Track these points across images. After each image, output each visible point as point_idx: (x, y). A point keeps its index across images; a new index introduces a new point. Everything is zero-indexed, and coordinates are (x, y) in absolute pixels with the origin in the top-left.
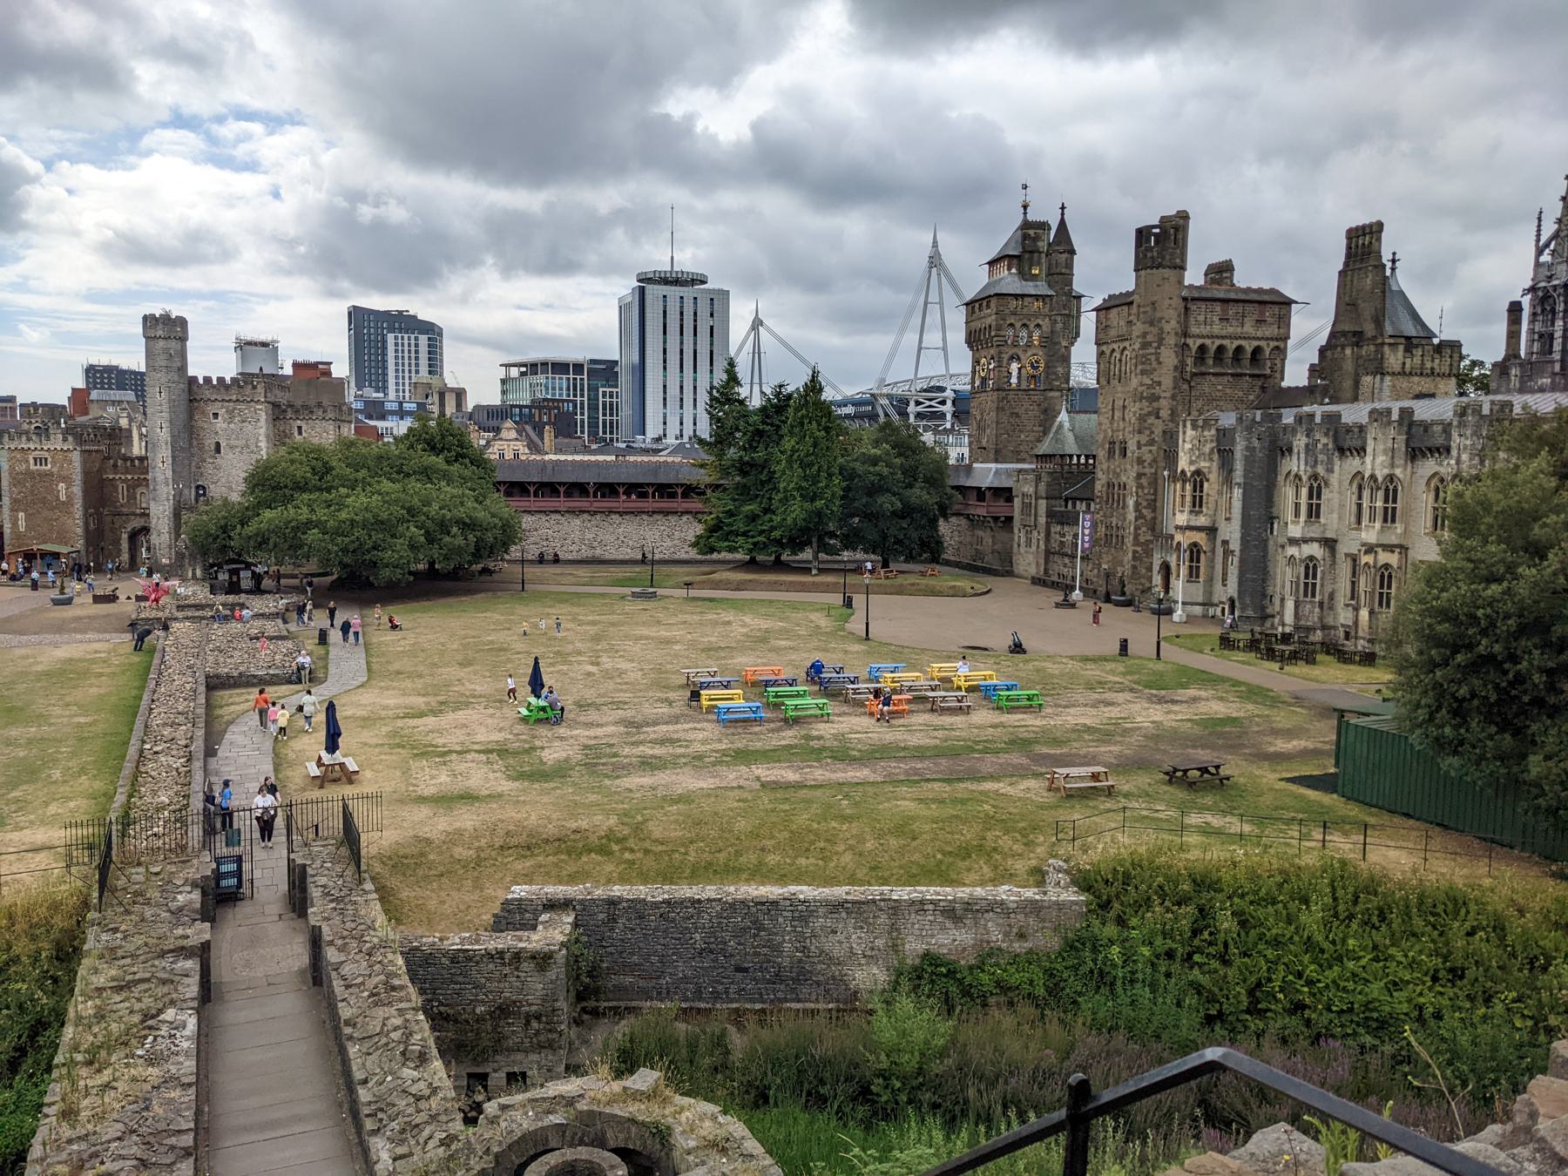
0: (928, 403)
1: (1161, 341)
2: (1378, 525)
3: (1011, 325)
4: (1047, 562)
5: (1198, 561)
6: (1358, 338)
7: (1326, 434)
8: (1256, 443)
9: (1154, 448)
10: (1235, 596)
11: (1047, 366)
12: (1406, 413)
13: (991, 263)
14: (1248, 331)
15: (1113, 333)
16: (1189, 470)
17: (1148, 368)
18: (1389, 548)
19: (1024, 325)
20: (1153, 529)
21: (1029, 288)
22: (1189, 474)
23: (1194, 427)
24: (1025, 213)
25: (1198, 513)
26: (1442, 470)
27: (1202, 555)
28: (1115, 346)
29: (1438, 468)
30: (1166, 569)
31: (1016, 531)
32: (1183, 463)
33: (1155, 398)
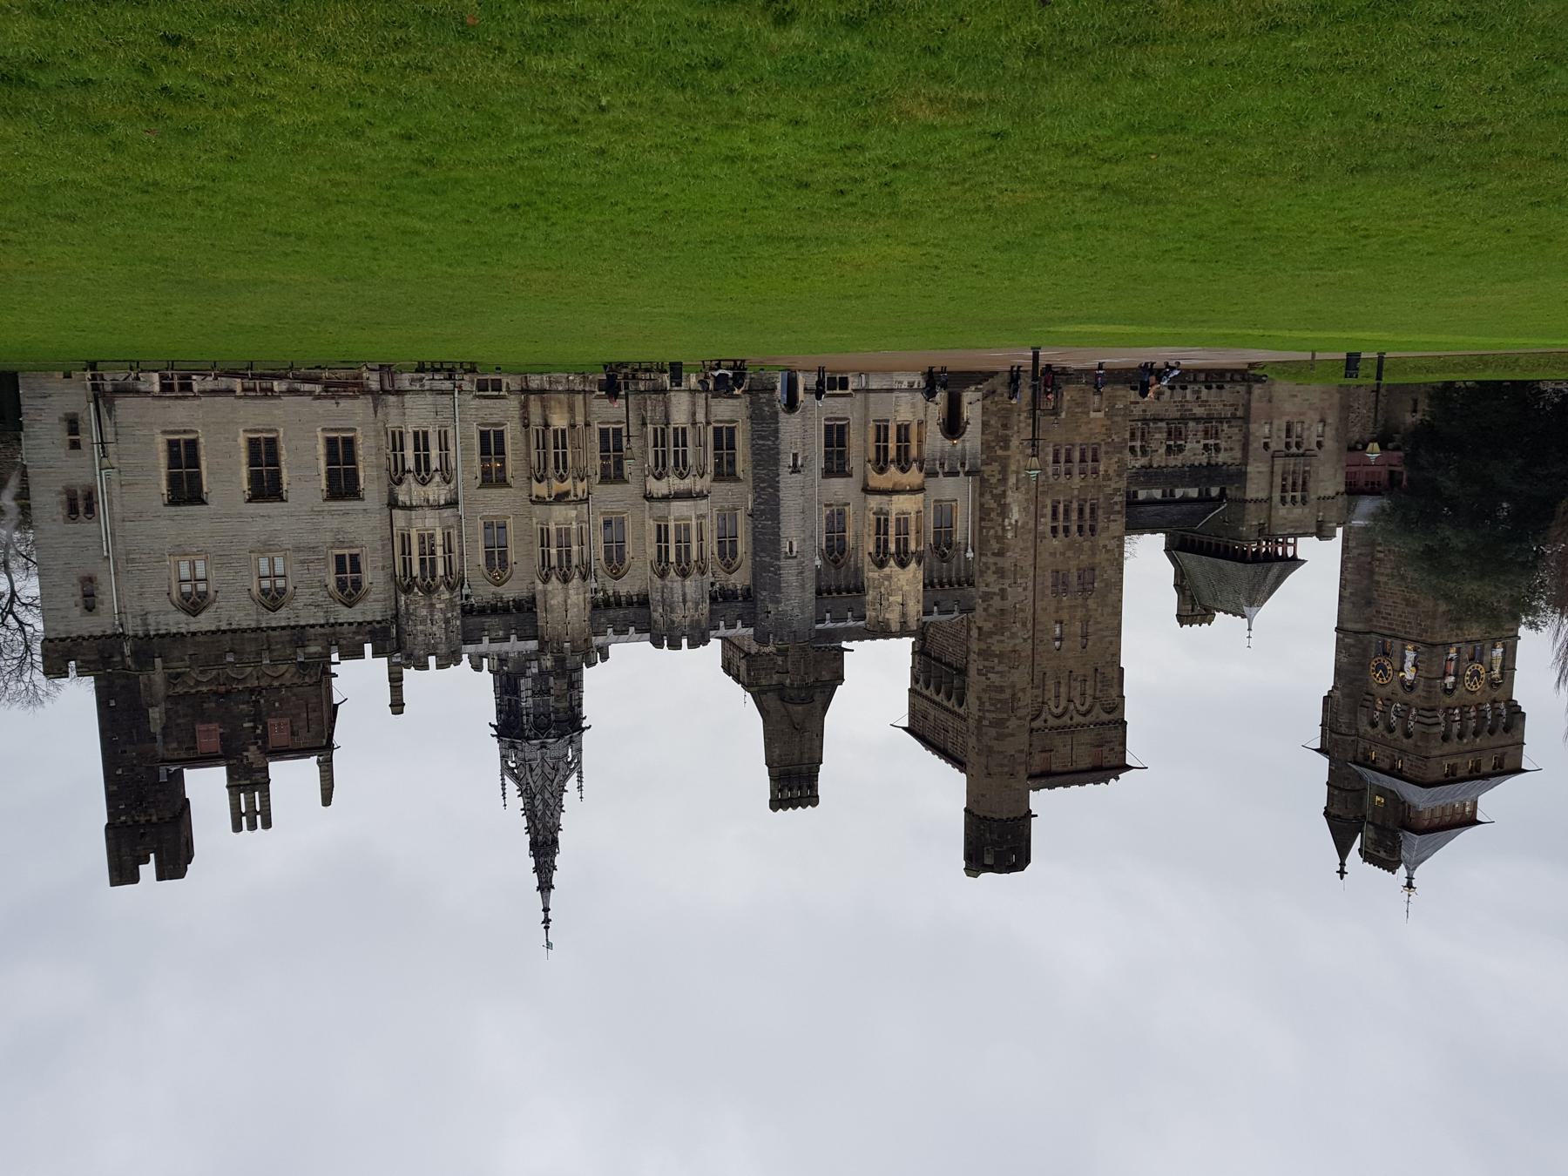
1: (979, 727)
2: (553, 528)
3: (1408, 735)
4: (1247, 407)
5: (878, 448)
7: (655, 622)
8: (771, 607)
9: (983, 589)
10: (783, 416)
11: (1364, 667)
13: (1472, 822)
17: (993, 694)
18: (540, 501)
19: (1391, 730)
20: (983, 480)
22: (892, 562)
24: (1410, 878)
25: (879, 512)
26: (493, 588)
27: (872, 455)
28: (1078, 719)
29: (498, 589)
30: (953, 426)
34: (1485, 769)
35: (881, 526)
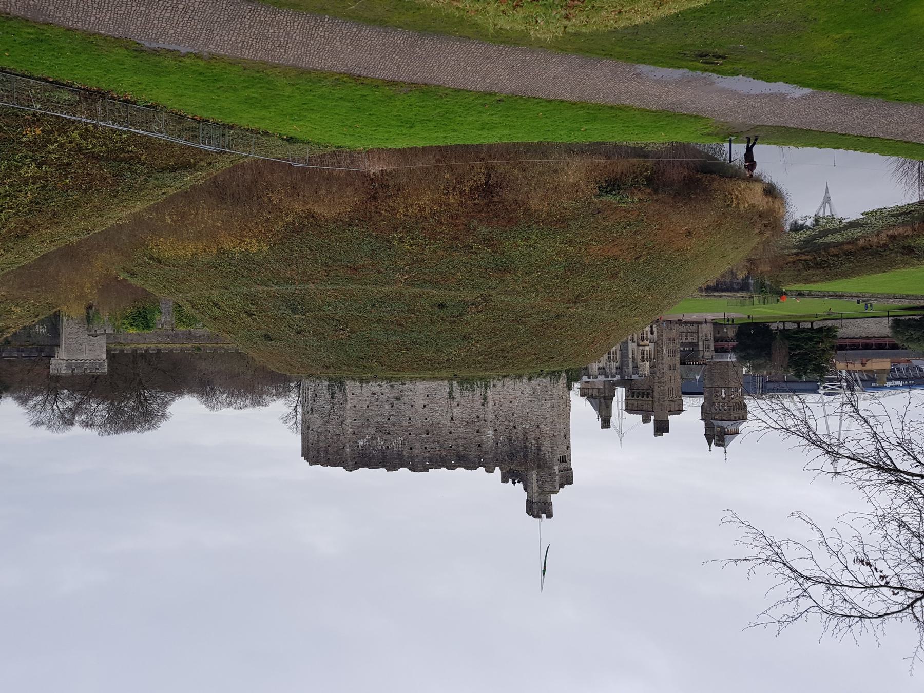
0: (834, 387)
4: (698, 330)
6: (605, 398)
12: (589, 378)
13: (738, 433)
14: (636, 401)
15: (676, 403)
16: (646, 362)
21: (720, 423)
23: (645, 374)
30: (652, 333)
31: (712, 339)
32: (648, 364)
33: (659, 383)
34: (741, 418)
35: (643, 353)
